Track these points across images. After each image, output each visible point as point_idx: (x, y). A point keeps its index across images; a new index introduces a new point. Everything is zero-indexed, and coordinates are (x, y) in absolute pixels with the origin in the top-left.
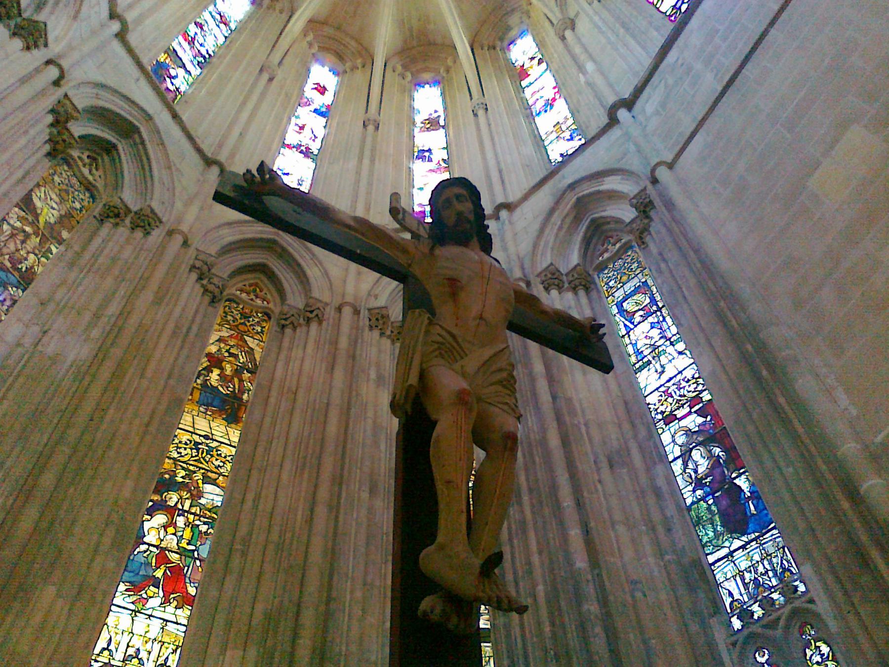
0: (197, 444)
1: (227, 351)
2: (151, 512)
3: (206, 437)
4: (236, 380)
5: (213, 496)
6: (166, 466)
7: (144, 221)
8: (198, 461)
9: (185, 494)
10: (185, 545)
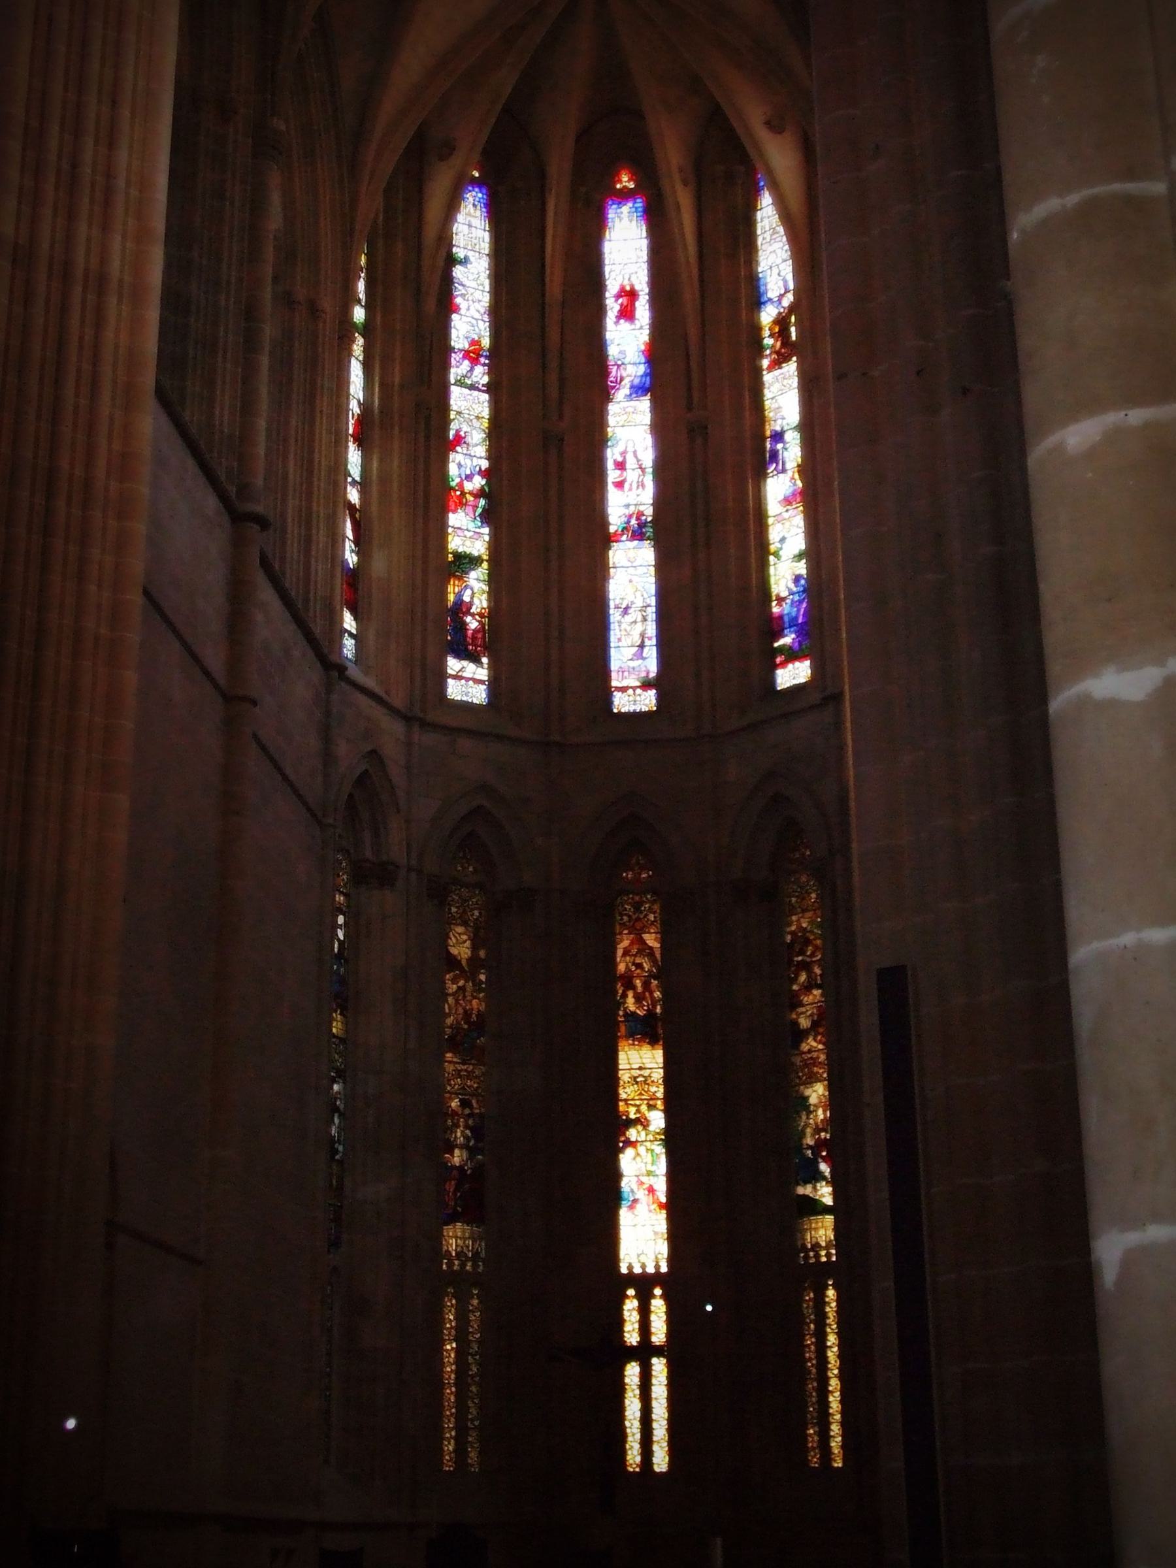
0: (635, 1078)
1: (634, 964)
2: (622, 1150)
3: (640, 1068)
4: (647, 994)
5: (657, 1120)
6: (621, 1109)
8: (641, 1094)
9: (640, 1128)
10: (650, 1168)
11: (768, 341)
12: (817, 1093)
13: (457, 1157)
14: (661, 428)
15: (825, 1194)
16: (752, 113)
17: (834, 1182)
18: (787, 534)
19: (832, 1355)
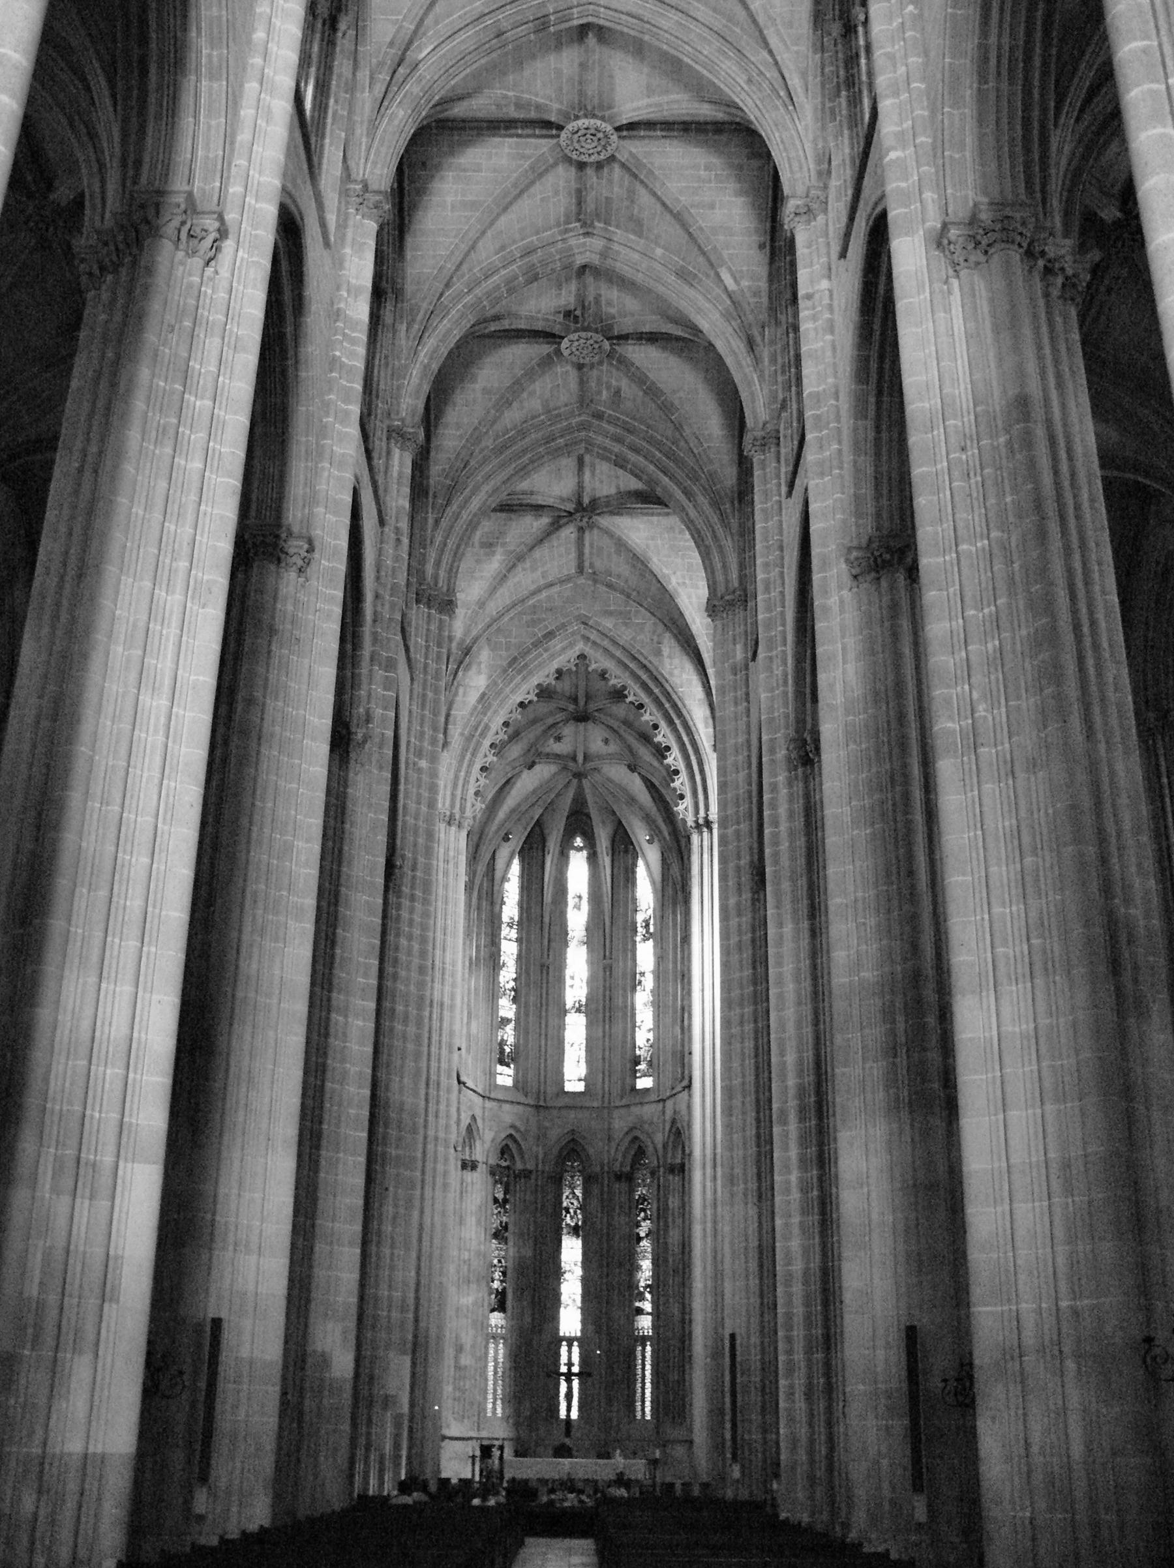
5: (579, 1271)
7: (526, 1174)
11: (640, 929)
12: (646, 1265)
13: (496, 1285)
14: (591, 963)
15: (647, 1306)
16: (641, 834)
17: (653, 1302)
18: (645, 1017)
19: (648, 1373)
